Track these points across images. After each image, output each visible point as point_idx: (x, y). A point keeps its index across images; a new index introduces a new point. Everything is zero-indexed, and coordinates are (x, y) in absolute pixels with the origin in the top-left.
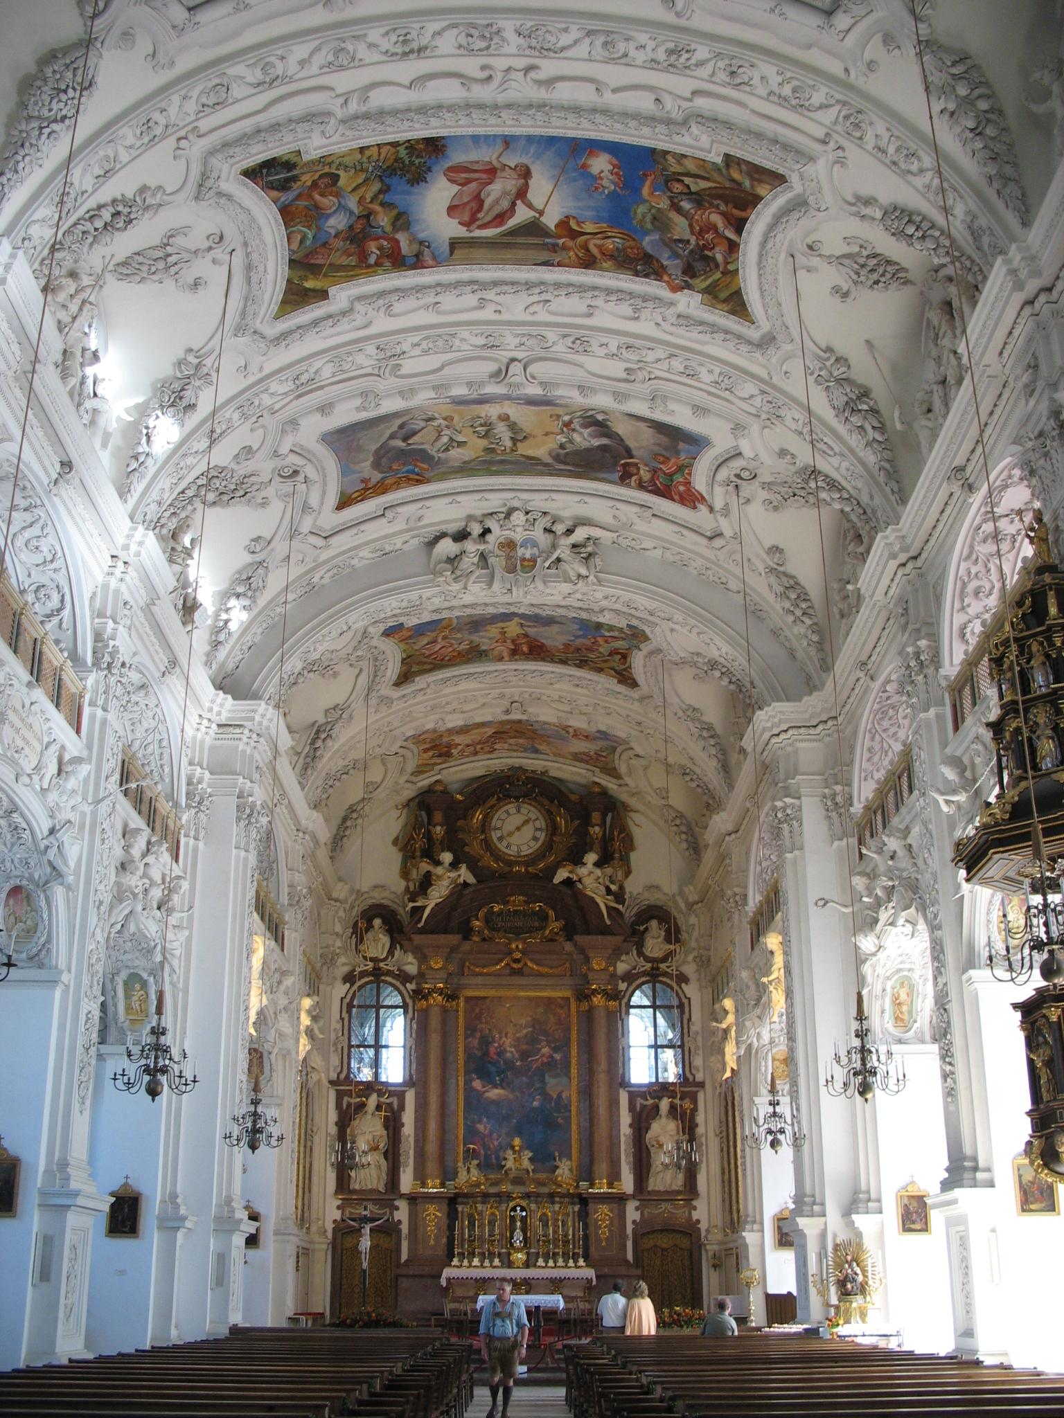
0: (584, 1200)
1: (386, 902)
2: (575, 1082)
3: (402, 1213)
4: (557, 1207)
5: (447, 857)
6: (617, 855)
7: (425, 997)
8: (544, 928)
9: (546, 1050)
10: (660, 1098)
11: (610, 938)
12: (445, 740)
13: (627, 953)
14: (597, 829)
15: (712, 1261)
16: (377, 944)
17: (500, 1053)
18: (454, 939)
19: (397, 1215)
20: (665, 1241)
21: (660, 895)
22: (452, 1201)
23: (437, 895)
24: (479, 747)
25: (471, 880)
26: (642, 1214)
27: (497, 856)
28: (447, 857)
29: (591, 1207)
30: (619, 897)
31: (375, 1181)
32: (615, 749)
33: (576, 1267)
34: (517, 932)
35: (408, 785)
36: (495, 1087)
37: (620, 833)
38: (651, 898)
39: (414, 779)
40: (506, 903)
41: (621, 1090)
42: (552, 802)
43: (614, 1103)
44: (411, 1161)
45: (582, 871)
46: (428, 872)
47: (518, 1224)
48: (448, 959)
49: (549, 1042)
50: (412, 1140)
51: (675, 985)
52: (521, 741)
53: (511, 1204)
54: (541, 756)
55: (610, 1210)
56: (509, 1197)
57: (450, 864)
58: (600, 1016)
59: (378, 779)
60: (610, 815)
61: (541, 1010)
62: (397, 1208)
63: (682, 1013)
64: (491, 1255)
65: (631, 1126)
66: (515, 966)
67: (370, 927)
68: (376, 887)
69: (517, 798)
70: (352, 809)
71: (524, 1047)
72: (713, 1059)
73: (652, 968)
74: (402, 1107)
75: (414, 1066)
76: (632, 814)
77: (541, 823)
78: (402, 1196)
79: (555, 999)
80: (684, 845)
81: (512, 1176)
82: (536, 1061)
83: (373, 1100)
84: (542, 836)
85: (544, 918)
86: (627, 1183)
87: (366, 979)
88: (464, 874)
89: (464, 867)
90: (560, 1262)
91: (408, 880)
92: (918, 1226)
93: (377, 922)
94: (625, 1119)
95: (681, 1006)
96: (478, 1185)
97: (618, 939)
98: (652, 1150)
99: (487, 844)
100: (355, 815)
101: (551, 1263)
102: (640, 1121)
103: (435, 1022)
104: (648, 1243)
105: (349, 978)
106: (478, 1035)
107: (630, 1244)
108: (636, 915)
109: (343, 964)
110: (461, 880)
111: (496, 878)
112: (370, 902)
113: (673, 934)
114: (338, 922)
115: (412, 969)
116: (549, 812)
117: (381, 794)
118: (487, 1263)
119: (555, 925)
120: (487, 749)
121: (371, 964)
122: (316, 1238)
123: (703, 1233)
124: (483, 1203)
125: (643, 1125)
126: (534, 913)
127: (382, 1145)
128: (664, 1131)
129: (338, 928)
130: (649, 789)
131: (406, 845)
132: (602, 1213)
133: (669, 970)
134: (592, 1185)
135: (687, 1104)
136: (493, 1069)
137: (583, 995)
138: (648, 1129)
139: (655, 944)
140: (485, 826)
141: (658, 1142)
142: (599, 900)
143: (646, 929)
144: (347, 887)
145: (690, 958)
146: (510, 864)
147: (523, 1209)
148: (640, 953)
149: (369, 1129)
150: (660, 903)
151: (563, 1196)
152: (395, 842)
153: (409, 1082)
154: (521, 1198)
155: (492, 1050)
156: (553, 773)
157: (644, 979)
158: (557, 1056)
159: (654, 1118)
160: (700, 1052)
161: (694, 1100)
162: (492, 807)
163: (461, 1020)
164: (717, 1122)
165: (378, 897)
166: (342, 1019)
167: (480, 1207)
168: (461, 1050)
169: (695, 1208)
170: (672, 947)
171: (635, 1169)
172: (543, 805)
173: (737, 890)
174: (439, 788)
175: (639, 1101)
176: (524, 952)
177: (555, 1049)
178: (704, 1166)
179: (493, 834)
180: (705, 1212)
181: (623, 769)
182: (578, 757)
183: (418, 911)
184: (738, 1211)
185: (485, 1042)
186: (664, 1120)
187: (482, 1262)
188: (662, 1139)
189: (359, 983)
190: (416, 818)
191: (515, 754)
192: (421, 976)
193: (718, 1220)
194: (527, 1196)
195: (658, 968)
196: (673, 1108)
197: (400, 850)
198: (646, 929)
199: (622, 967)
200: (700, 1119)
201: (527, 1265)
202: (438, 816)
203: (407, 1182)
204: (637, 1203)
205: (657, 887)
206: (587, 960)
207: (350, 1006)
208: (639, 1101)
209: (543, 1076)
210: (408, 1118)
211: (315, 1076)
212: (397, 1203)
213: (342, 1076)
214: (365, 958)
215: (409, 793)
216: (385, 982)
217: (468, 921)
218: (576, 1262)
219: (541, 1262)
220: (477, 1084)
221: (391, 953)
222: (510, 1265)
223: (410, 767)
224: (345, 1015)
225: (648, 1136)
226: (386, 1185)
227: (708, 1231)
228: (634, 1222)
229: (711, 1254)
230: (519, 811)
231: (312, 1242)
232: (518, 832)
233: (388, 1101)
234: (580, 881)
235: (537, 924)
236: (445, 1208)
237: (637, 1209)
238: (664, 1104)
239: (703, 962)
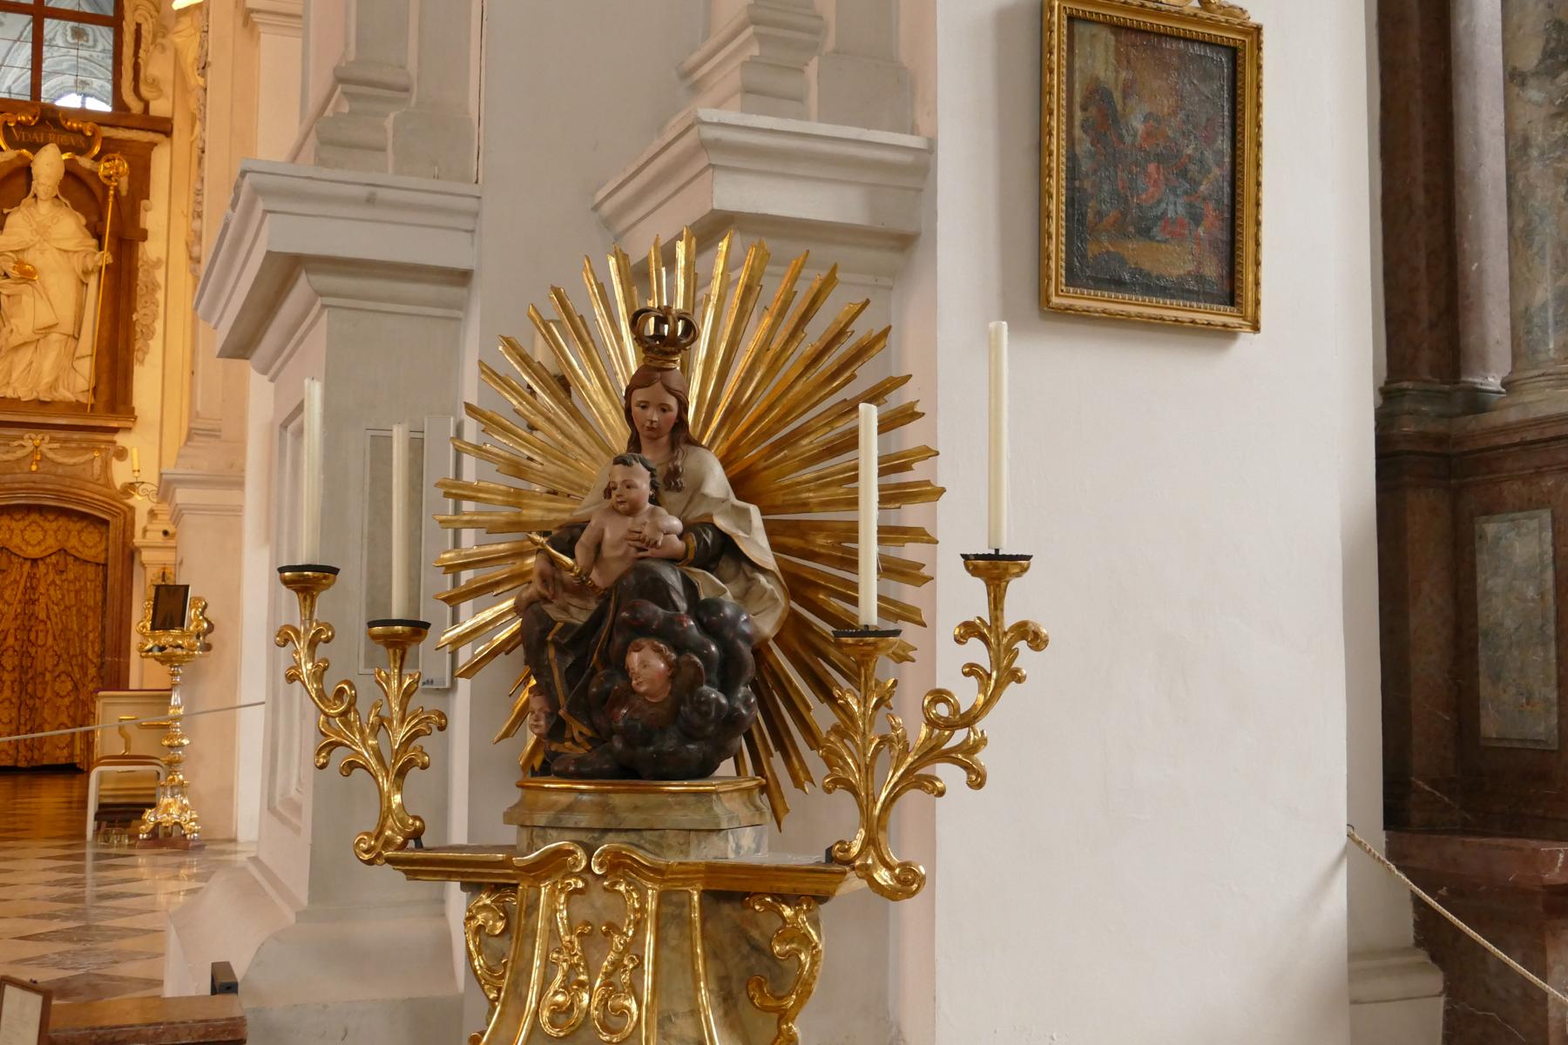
10: (35, 147)
92: (1174, 261)
123: (141, 520)
135: (113, 170)
141: (20, 264)
159: (16, 203)
169: (122, 454)
178: (155, 344)
186: (44, 208)
188: (33, 258)
200: (154, 217)
238: (48, 163)
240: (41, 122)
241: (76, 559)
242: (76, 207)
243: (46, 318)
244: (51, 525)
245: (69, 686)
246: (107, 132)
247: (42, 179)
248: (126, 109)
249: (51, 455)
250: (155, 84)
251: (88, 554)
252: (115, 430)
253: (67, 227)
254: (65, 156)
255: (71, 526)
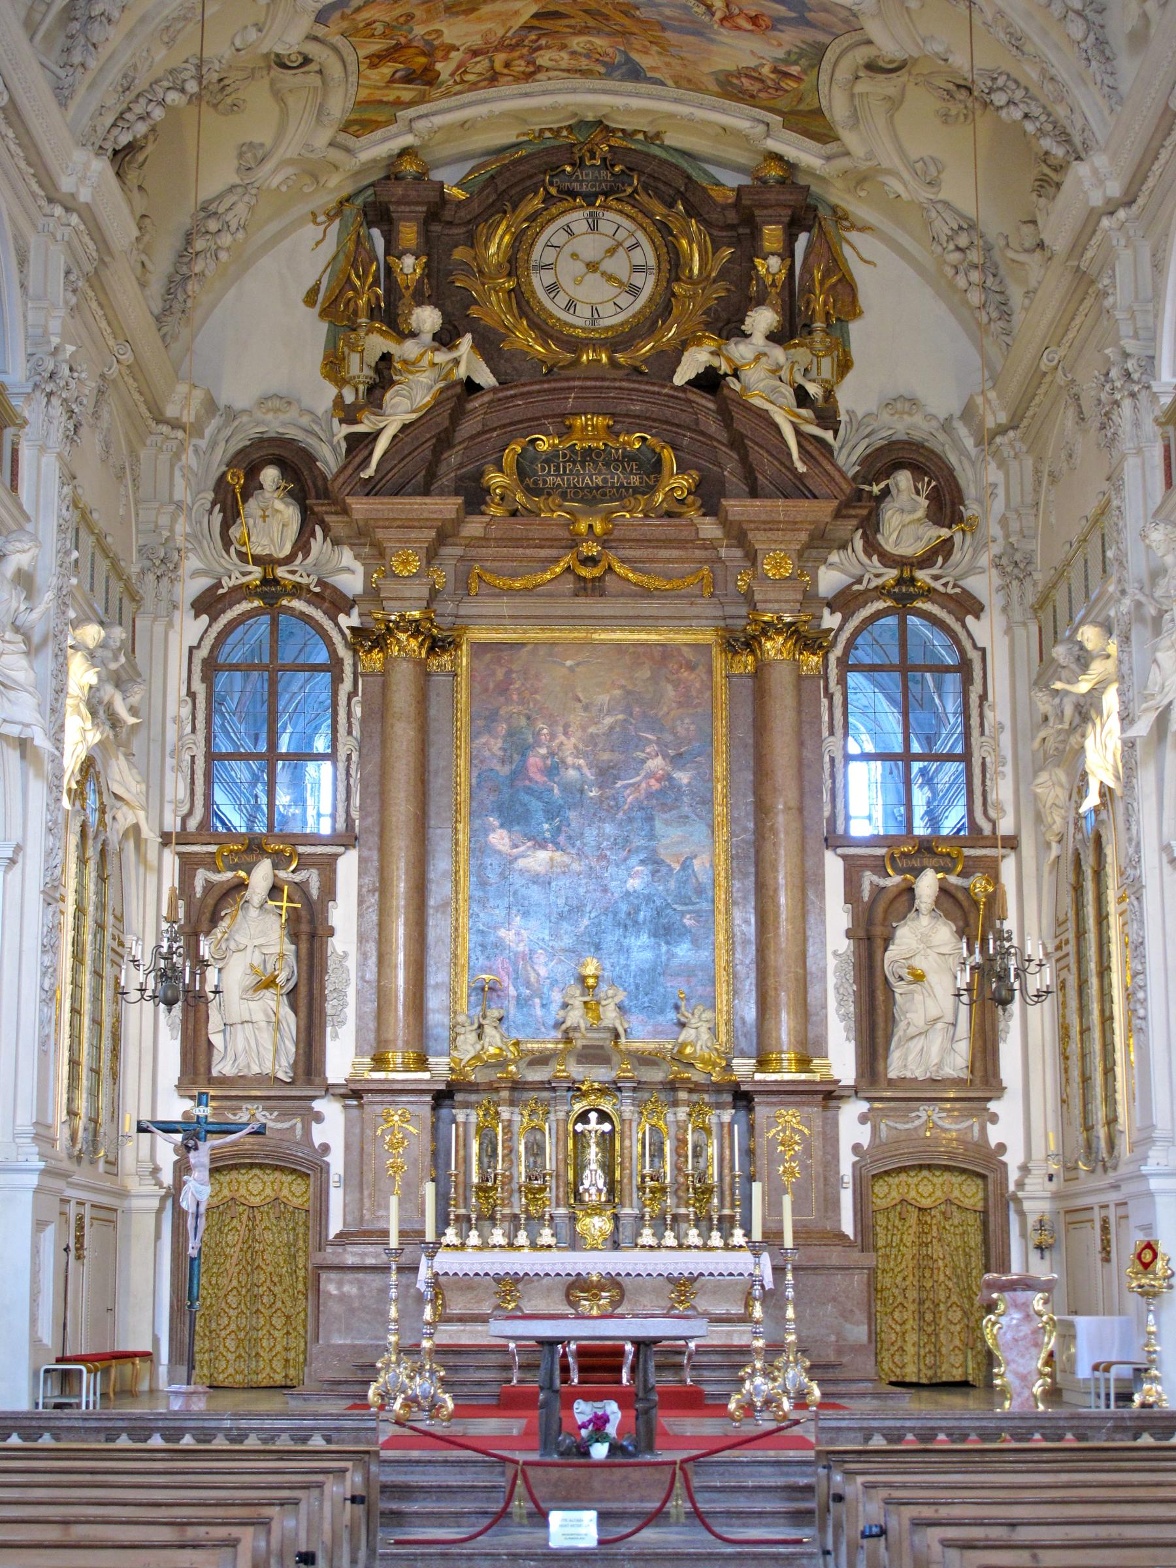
0: (743, 1098)
1: (292, 433)
2: (722, 834)
3: (331, 1126)
4: (682, 1112)
5: (427, 318)
6: (819, 325)
7: (379, 643)
8: (651, 490)
9: (656, 764)
10: (917, 872)
11: (806, 504)
12: (419, 30)
13: (843, 547)
14: (774, 262)
15: (1034, 1238)
16: (273, 521)
17: (552, 771)
18: (446, 506)
19: (319, 1134)
20: (926, 1190)
21: (918, 419)
22: (443, 1097)
23: (403, 406)
24: (500, 58)
25: (485, 378)
26: (875, 1131)
27: (544, 328)
28: (427, 318)
29: (761, 1112)
30: (827, 417)
31: (269, 1056)
32: (820, 51)
33: (727, 1247)
34: (591, 497)
35: (335, 155)
36: (541, 845)
37: (826, 275)
38: (899, 427)
39: (350, 141)
40: (566, 431)
41: (829, 856)
42: (671, 205)
43: (809, 882)
44: (350, 1012)
45: (741, 351)
46: (386, 358)
47: (593, 1153)
48: (431, 555)
49: (662, 745)
50: (351, 964)
51: (950, 620)
52: (600, 42)
53: (578, 1107)
54: (643, 87)
55: (807, 1121)
56: (576, 1090)
57: (436, 337)
58: (781, 682)
59: (264, 136)
60: (803, 239)
61: (645, 673)
62: (319, 1118)
63: (967, 681)
64: (535, 1221)
65: (849, 934)
66: (585, 572)
67: (252, 486)
68: (263, 400)
69: (590, 199)
70: (207, 210)
71: (606, 756)
72: (1043, 777)
73: (900, 581)
74: (329, 891)
75: (356, 800)
76: (853, 236)
77: (646, 254)
78: (328, 1090)
79: (677, 648)
80: (975, 297)
81: (579, 1043)
82: (632, 788)
83: (261, 875)
84: (648, 284)
85: (657, 466)
86: (841, 1061)
87: (245, 606)
88: (467, 360)
89: (466, 343)
90: (693, 1236)
91: (341, 382)
93: (270, 475)
94: (837, 917)
95: (964, 667)
96: (502, 1063)
97: (822, 510)
98: (899, 988)
99: (521, 301)
100: (213, 225)
101: (670, 1239)
102: (870, 922)
103: (402, 697)
104: (886, 1193)
105: (209, 603)
106: (502, 728)
107: (847, 1198)
108: (867, 461)
109: (195, 574)
110: (461, 372)
111: (542, 378)
112: (254, 431)
113: (946, 505)
114: (187, 476)
115: (351, 579)
116: (664, 228)
117: (272, 176)
118: (522, 1238)
119: (680, 483)
120: (520, 66)
121: (256, 573)
122: (133, 1185)
123: (1013, 1175)
124: (512, 1103)
125: (878, 930)
126: (629, 458)
127: (281, 978)
128: (927, 945)
129: (181, 492)
130: (898, 164)
131: (335, 302)
132: (783, 1124)
133: (938, 585)
134: (763, 1064)
135: (979, 885)
136: (536, 805)
137: (739, 642)
138: (888, 940)
139: (905, 524)
140: (514, 263)
142: (780, 418)
143: (886, 492)
144: (198, 394)
145: (984, 560)
146: (575, 345)
147: (604, 1117)
148: (872, 547)
149: (254, 939)
150: (917, 436)
151: (695, 1088)
152: (311, 298)
153: (347, 838)
154: (603, 1092)
155: (533, 761)
156: (672, 139)
157: (880, 605)
158: (683, 777)
160: (1008, 769)
161: (994, 877)
162: (532, 218)
163: (463, 697)
164: (1047, 921)
165: (275, 424)
166: (191, 694)
167: (505, 1112)
168: (462, 762)
169: (994, 1118)
170: (945, 533)
171: (859, 1032)
172: (648, 214)
173: (1130, 345)
174: (409, 168)
175: (869, 879)
176: (605, 542)
177: (678, 760)
179: (535, 279)
180: (1021, 1128)
181: (838, 109)
182: (733, 87)
183: (360, 444)
184: (1112, 1121)
185: (518, 747)
186: (925, 920)
187: (511, 1236)
188: (920, 963)
189: (230, 615)
190: (358, 242)
191: (579, 82)
192: (373, 594)
193: (1047, 1140)
194: (612, 1089)
195: (912, 580)
196: (944, 891)
197: (324, 314)
198: (886, 492)
199: (829, 580)
201: (616, 1245)
202: (409, 234)
203: (341, 1059)
204: (864, 1106)
205: (913, 402)
206: (752, 557)
207: (211, 667)
208: (869, 879)
209: (650, 819)
210: (344, 917)
211: (125, 818)
212: (317, 1105)
213: (193, 824)
214: (242, 556)
215: (337, 185)
216: (290, 611)
217: (480, 474)
218: (727, 1235)
219: (647, 1237)
220: (499, 839)
221: (302, 545)
222: (575, 1242)
223: (339, 105)
224: (199, 687)
225: (893, 953)
226: (294, 1067)
227: (1025, 1169)
228: (856, 1148)
229: (1032, 1220)
230: (594, 228)
231: (123, 1194)
232: (591, 272)
233: (298, 877)
234: (736, 375)
235: (635, 480)
236: (426, 1111)
237: (863, 1119)
238: (927, 884)
239: (1014, 567)
240: (918, 851)
241: (959, 1207)
242: (948, 916)
243: (934, 1012)
244: (940, 1179)
245: (959, 1314)
246: (967, 852)
247: (925, 899)
248: (980, 830)
249: (940, 1123)
250: (999, 807)
251: (967, 1203)
252: (989, 1099)
253: (944, 933)
254: (940, 875)
255: (954, 1179)
